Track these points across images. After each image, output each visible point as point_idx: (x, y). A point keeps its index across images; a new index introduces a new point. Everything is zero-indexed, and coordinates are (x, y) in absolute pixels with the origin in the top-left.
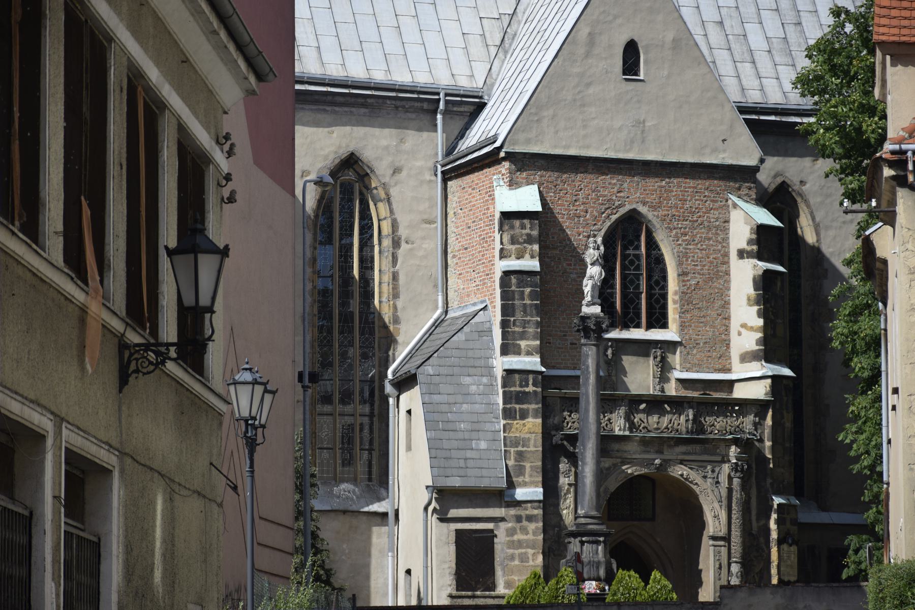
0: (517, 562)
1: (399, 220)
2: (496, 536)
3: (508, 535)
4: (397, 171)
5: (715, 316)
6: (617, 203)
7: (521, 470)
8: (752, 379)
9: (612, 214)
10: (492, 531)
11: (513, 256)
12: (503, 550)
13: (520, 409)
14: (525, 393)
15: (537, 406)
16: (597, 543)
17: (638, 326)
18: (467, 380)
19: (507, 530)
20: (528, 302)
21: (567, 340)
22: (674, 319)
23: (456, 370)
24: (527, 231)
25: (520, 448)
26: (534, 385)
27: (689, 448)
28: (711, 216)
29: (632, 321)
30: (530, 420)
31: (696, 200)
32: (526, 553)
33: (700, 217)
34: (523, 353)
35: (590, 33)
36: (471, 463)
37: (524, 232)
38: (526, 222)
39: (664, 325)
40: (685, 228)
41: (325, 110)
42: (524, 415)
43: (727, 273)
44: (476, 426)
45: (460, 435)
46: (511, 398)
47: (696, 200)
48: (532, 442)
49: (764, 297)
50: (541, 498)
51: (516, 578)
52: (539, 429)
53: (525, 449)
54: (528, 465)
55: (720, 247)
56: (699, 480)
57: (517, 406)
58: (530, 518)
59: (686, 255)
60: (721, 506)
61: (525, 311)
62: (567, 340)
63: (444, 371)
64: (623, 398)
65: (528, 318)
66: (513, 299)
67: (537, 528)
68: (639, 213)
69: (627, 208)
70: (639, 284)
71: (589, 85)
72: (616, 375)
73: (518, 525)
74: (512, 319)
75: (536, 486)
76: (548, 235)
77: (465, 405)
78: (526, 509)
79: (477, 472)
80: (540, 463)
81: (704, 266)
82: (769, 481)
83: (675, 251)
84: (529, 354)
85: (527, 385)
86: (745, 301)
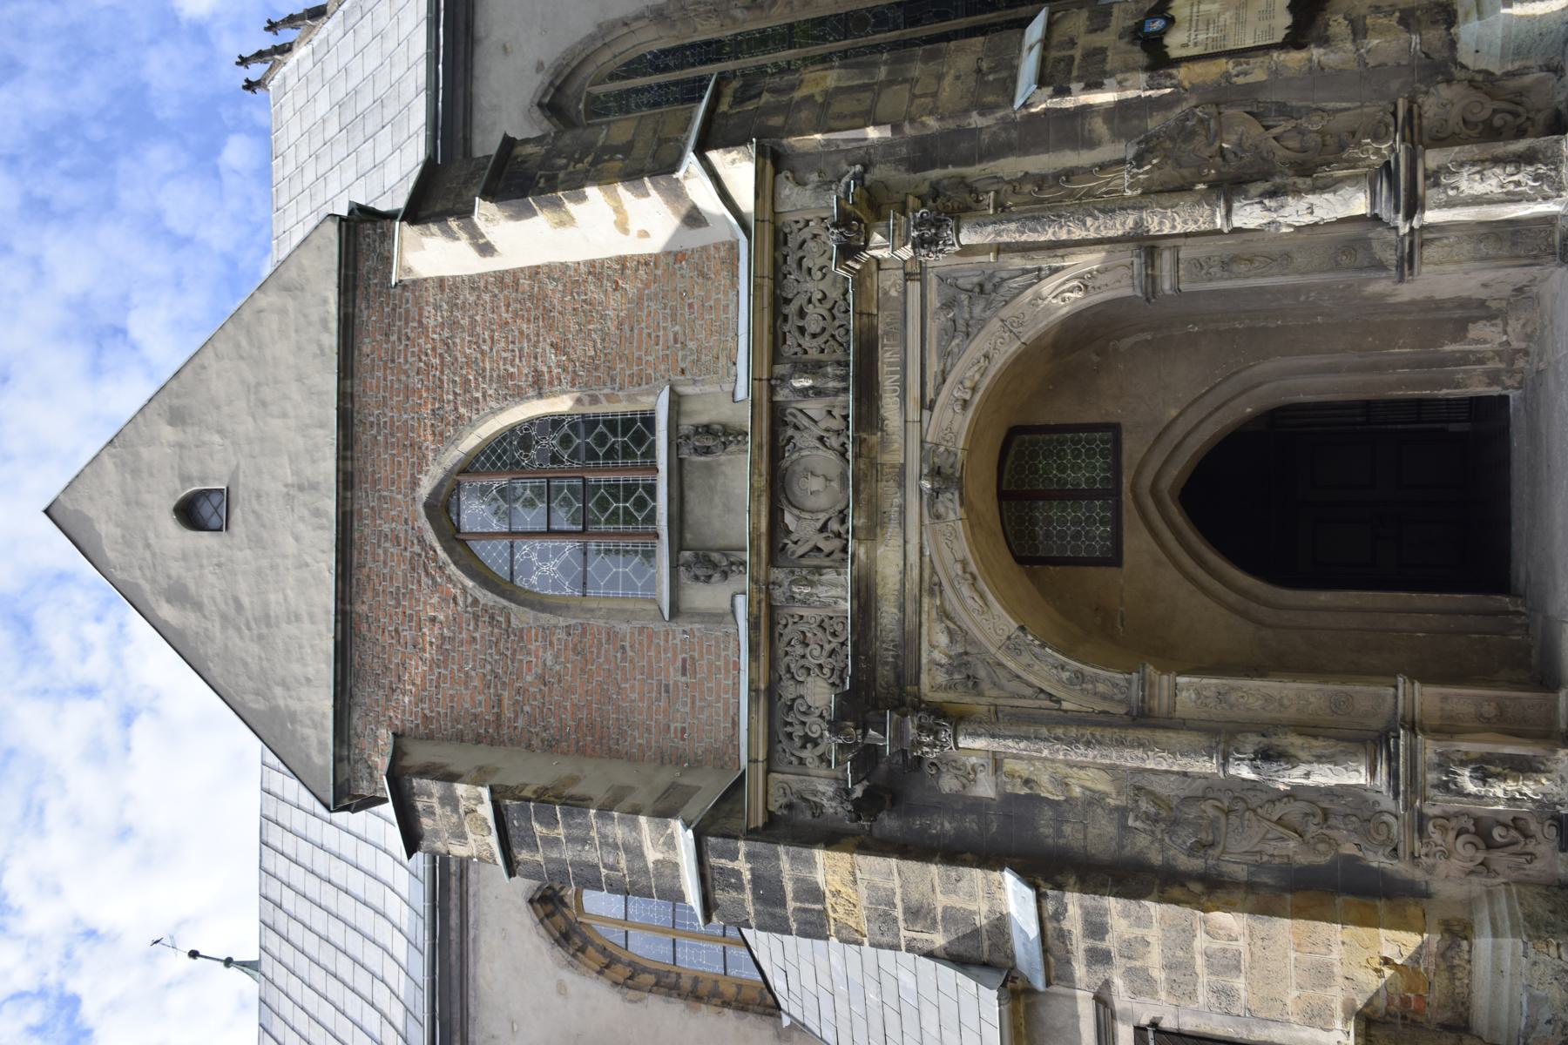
0: (1240, 983)
2: (1154, 1024)
3: (1153, 993)
5: (618, 294)
6: (417, 549)
9: (435, 560)
10: (1139, 1030)
12: (1197, 1013)
13: (796, 899)
14: (756, 880)
15: (784, 857)
19: (1136, 993)
20: (561, 831)
21: (676, 683)
22: (631, 398)
25: (899, 913)
26: (734, 856)
28: (432, 323)
30: (820, 877)
31: (406, 361)
32: (1208, 955)
33: (434, 349)
34: (671, 856)
35: (169, 601)
37: (438, 810)
39: (649, 421)
40: (454, 382)
41: (475, 940)
42: (812, 893)
43: (535, 272)
46: (773, 916)
47: (406, 361)
49: (542, 192)
51: (1295, 993)
53: (898, 900)
55: (487, 297)
57: (791, 905)
58: (1096, 929)
60: (1056, 270)
62: (676, 683)
65: (593, 834)
67: (1126, 914)
68: (435, 494)
69: (423, 523)
71: (239, 606)
73: (1117, 960)
74: (604, 871)
75: (1000, 886)
78: (1063, 936)
81: (521, 332)
82: (976, 120)
83: (493, 404)
84: (671, 843)
85: (737, 874)
86: (567, 232)
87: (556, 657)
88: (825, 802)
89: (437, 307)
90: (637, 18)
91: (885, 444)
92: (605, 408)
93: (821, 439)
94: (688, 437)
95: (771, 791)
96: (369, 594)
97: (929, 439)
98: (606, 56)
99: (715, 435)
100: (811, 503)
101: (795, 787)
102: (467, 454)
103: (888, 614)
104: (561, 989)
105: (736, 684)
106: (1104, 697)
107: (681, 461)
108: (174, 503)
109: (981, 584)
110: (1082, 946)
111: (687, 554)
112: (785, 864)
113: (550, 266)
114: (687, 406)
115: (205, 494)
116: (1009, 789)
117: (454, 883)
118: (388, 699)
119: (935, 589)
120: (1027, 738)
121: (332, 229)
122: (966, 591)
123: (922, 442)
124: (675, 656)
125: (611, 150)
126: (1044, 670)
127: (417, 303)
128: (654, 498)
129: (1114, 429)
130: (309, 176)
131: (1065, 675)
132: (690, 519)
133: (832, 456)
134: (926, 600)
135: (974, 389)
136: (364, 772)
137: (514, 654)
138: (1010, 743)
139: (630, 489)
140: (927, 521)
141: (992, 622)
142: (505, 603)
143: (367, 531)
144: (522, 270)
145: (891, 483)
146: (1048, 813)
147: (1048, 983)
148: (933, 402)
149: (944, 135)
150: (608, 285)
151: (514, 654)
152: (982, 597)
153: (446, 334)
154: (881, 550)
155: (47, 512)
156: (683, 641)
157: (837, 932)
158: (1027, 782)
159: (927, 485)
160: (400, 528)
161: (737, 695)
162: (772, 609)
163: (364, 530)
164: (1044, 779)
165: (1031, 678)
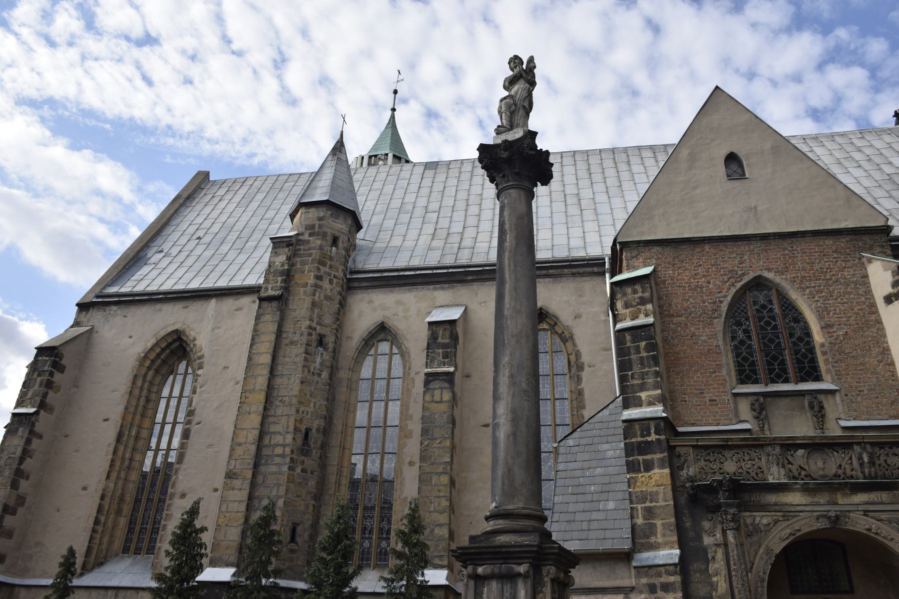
1: (581, 350)
5: (876, 363)
6: (740, 273)
7: (651, 529)
9: (736, 282)
11: (628, 319)
14: (647, 442)
15: (662, 455)
16: (511, 578)
17: (786, 381)
18: (606, 446)
20: (644, 354)
22: (828, 371)
23: (596, 440)
24: (640, 294)
25: (648, 504)
26: (657, 433)
27: (873, 496)
28: (846, 274)
30: (656, 471)
34: (645, 404)
35: (690, 154)
36: (594, 525)
37: (636, 296)
38: (638, 287)
39: (818, 378)
42: (649, 467)
43: (879, 322)
44: (606, 488)
45: (589, 497)
46: (633, 450)
48: (661, 496)
50: (677, 560)
52: (668, 481)
53: (653, 504)
54: (659, 523)
55: (863, 299)
57: (640, 458)
58: (666, 588)
61: (642, 364)
63: (583, 442)
65: (647, 369)
66: (629, 354)
69: (752, 275)
70: (779, 343)
71: (695, 188)
72: (770, 430)
74: (630, 373)
76: (670, 305)
77: (599, 470)
78: (659, 575)
79: (601, 534)
80: (673, 520)
81: (850, 317)
83: (813, 306)
84: (650, 404)
85: (649, 435)
87: (705, 341)
88: (685, 471)
89: (854, 275)
91: (845, 495)
92: (821, 359)
93: (840, 466)
94: (816, 398)
95: (685, 448)
96: (714, 251)
97: (851, 514)
99: (820, 411)
100: (812, 462)
101: (689, 458)
102: (787, 294)
103: (772, 498)
105: (710, 425)
106: (756, 590)
107: (804, 395)
108: (735, 151)
109: (792, 538)
110: (656, 582)
111: (762, 399)
112: (658, 456)
113: (883, 329)
114: (829, 397)
115: (741, 166)
116: (709, 550)
117: (544, 272)
118: (669, 263)
119: (786, 518)
120: (739, 560)
121: (880, 223)
122: (788, 531)
123: (849, 511)
124: (717, 396)
126: (762, 565)
127: (854, 265)
128: (783, 382)
129: (851, 591)
130: (857, 156)
131: (761, 574)
132: (777, 400)
133: (834, 471)
134: (781, 514)
135: (877, 534)
136: (634, 254)
137: (703, 321)
138: (735, 552)
139: (785, 371)
140: (815, 514)
141: (776, 542)
142: (724, 316)
143: (742, 248)
144: (879, 316)
145: (828, 498)
146: (703, 567)
147: (635, 567)
148: (867, 516)
150: (880, 358)
151: (703, 321)
152: (787, 538)
153: (842, 281)
154: (798, 494)
155: (717, 87)
156: (724, 400)
157: (632, 478)
158: (714, 558)
159: (830, 514)
160: (747, 264)
161: (706, 425)
162: (762, 446)
163: (744, 247)
164: (716, 566)
165: (757, 560)
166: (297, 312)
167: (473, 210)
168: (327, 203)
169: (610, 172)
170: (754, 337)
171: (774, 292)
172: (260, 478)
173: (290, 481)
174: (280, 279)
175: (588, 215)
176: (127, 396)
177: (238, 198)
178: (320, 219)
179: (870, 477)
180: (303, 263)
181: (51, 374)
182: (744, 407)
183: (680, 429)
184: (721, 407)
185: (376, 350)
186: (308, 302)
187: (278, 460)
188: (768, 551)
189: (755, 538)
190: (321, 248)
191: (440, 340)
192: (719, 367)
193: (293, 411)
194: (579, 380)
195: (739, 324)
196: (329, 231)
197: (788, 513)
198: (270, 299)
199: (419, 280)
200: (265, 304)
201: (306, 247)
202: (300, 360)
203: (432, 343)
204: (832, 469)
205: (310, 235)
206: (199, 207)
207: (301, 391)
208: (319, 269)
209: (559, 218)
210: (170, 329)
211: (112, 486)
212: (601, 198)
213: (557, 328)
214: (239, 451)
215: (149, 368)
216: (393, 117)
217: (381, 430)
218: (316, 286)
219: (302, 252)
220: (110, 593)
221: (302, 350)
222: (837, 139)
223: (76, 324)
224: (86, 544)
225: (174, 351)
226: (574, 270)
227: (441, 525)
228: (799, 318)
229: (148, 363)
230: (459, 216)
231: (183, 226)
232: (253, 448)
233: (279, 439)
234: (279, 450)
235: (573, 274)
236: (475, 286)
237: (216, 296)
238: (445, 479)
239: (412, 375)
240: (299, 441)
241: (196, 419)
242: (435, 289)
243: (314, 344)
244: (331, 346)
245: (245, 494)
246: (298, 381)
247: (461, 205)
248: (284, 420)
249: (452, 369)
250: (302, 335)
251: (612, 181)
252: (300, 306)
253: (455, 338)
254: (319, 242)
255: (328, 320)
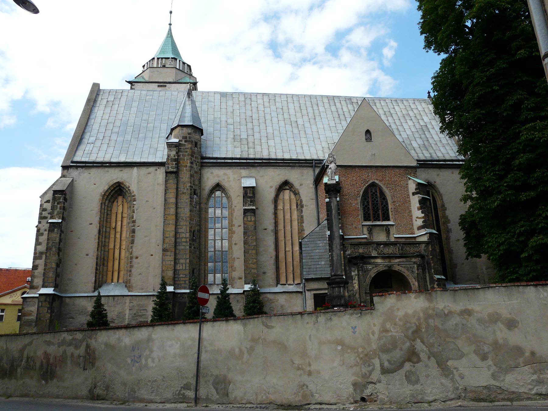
4: (301, 185)
8: (422, 235)
16: (340, 287)
17: (379, 220)
22: (392, 218)
23: (315, 239)
29: (377, 219)
36: (318, 269)
39: (389, 220)
44: (321, 257)
56: (406, 271)
59: (394, 196)
63: (310, 240)
64: (374, 243)
69: (371, 181)
79: (320, 272)
82: (433, 270)
86: (417, 209)
90: (443, 202)
98: (436, 194)
103: (372, 261)
104: (271, 187)
115: (371, 136)
117: (288, 164)
125: (428, 217)
126: (368, 280)
139: (379, 217)
141: (373, 274)
149: (431, 266)
163: (369, 170)
166: (184, 179)
167: (250, 125)
168: (192, 126)
169: (310, 110)
170: (370, 203)
171: (378, 188)
172: (177, 251)
173: (190, 252)
174: (174, 163)
175: (302, 133)
176: (99, 213)
177: (123, 103)
178: (189, 134)
179: (401, 254)
180: (184, 155)
181: (64, 204)
182: (365, 230)
183: (345, 237)
184: (358, 230)
185: (215, 195)
186: (188, 175)
187: (184, 244)
188: (370, 276)
189: (367, 273)
190: (191, 149)
191: (248, 195)
192: (358, 215)
193: (188, 223)
194: (302, 211)
195: (365, 199)
196: (193, 140)
197: (377, 265)
198: (171, 173)
199: (234, 165)
200: (169, 175)
201: (184, 148)
202: (188, 201)
203: (245, 196)
204: (390, 251)
205: (185, 142)
206: (102, 107)
207: (190, 215)
208: (191, 159)
209: (290, 134)
210: (115, 181)
211: (99, 254)
212: (307, 125)
213: (292, 189)
214: (167, 240)
215: (106, 200)
216: (170, 30)
217: (220, 230)
218: (191, 167)
219: (182, 150)
220: (110, 298)
221: (189, 197)
222: (404, 102)
223: (63, 176)
224: (94, 278)
225: (117, 191)
226: (300, 165)
227: (254, 269)
228: (384, 198)
229: (105, 197)
230: (243, 128)
231: (98, 120)
232: (173, 239)
233: (183, 235)
234: (184, 240)
235: (300, 166)
236: (258, 168)
237: (137, 166)
238: (254, 252)
239: (233, 207)
240: (192, 235)
241: (137, 224)
242: (241, 169)
243: (193, 194)
244: (199, 194)
245: (172, 258)
246: (188, 211)
247: (243, 121)
248: (184, 227)
249: (254, 208)
250: (187, 190)
251: (311, 115)
252: (185, 176)
253: (254, 194)
254: (190, 146)
255: (197, 183)
